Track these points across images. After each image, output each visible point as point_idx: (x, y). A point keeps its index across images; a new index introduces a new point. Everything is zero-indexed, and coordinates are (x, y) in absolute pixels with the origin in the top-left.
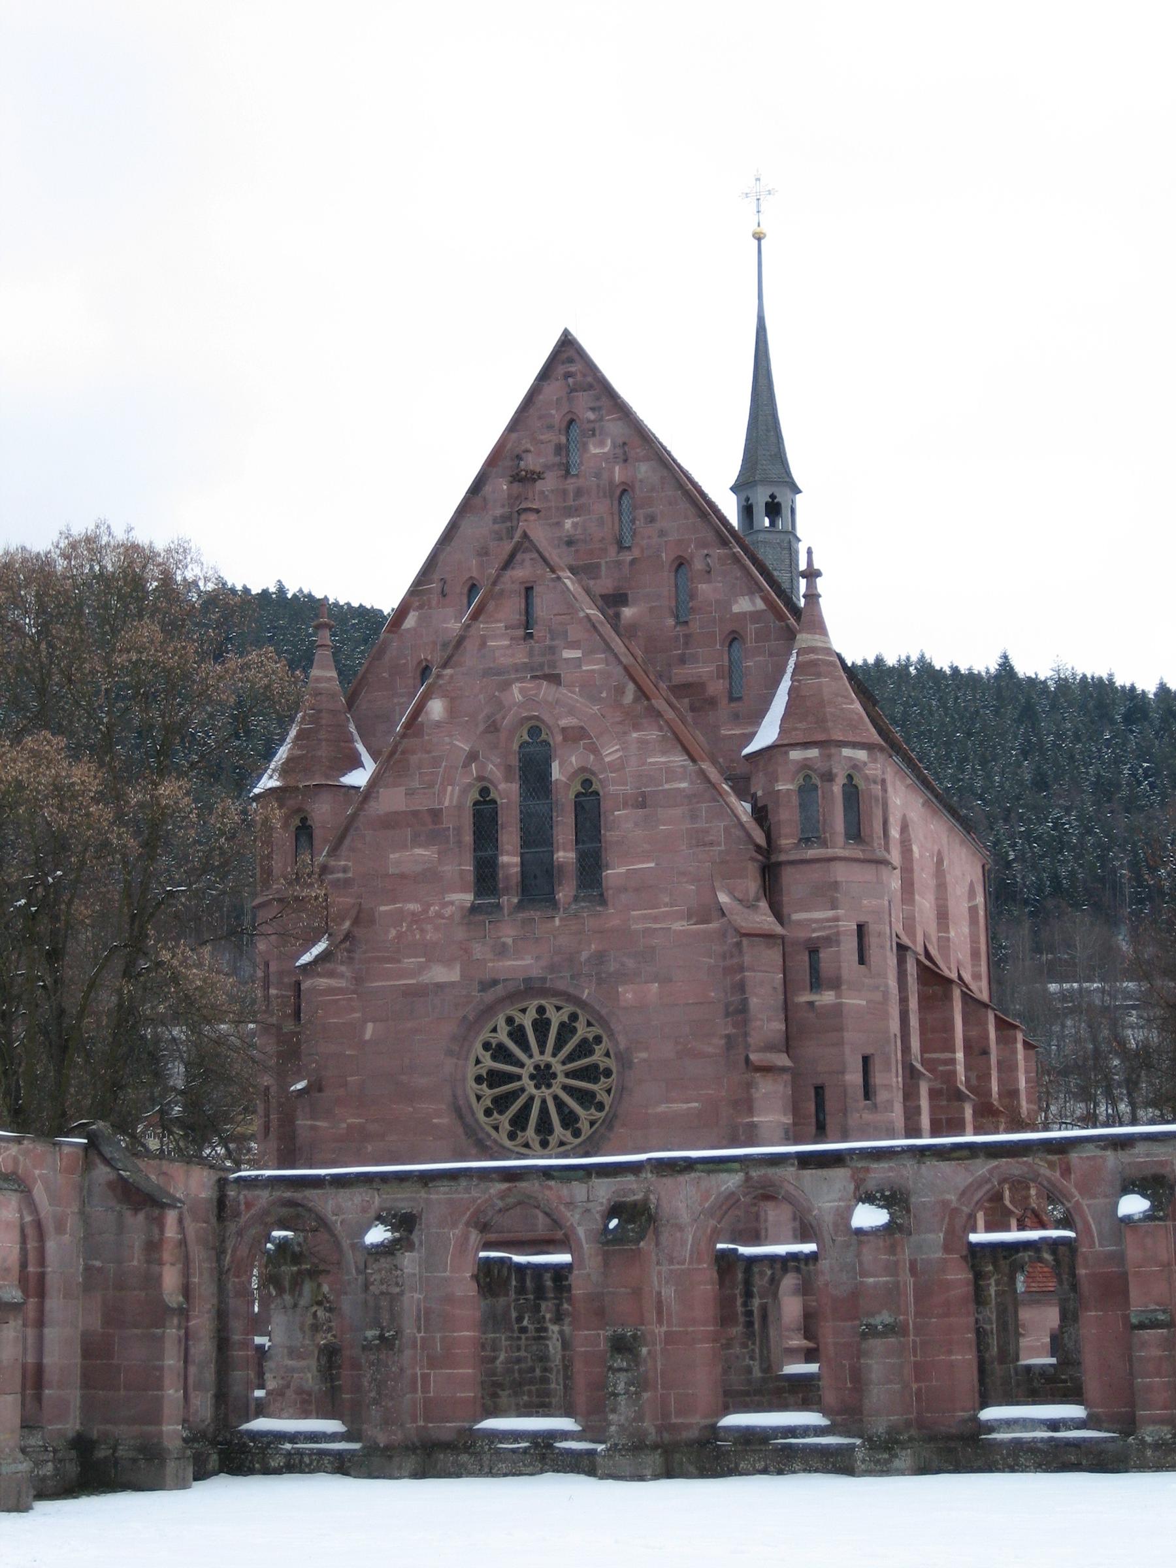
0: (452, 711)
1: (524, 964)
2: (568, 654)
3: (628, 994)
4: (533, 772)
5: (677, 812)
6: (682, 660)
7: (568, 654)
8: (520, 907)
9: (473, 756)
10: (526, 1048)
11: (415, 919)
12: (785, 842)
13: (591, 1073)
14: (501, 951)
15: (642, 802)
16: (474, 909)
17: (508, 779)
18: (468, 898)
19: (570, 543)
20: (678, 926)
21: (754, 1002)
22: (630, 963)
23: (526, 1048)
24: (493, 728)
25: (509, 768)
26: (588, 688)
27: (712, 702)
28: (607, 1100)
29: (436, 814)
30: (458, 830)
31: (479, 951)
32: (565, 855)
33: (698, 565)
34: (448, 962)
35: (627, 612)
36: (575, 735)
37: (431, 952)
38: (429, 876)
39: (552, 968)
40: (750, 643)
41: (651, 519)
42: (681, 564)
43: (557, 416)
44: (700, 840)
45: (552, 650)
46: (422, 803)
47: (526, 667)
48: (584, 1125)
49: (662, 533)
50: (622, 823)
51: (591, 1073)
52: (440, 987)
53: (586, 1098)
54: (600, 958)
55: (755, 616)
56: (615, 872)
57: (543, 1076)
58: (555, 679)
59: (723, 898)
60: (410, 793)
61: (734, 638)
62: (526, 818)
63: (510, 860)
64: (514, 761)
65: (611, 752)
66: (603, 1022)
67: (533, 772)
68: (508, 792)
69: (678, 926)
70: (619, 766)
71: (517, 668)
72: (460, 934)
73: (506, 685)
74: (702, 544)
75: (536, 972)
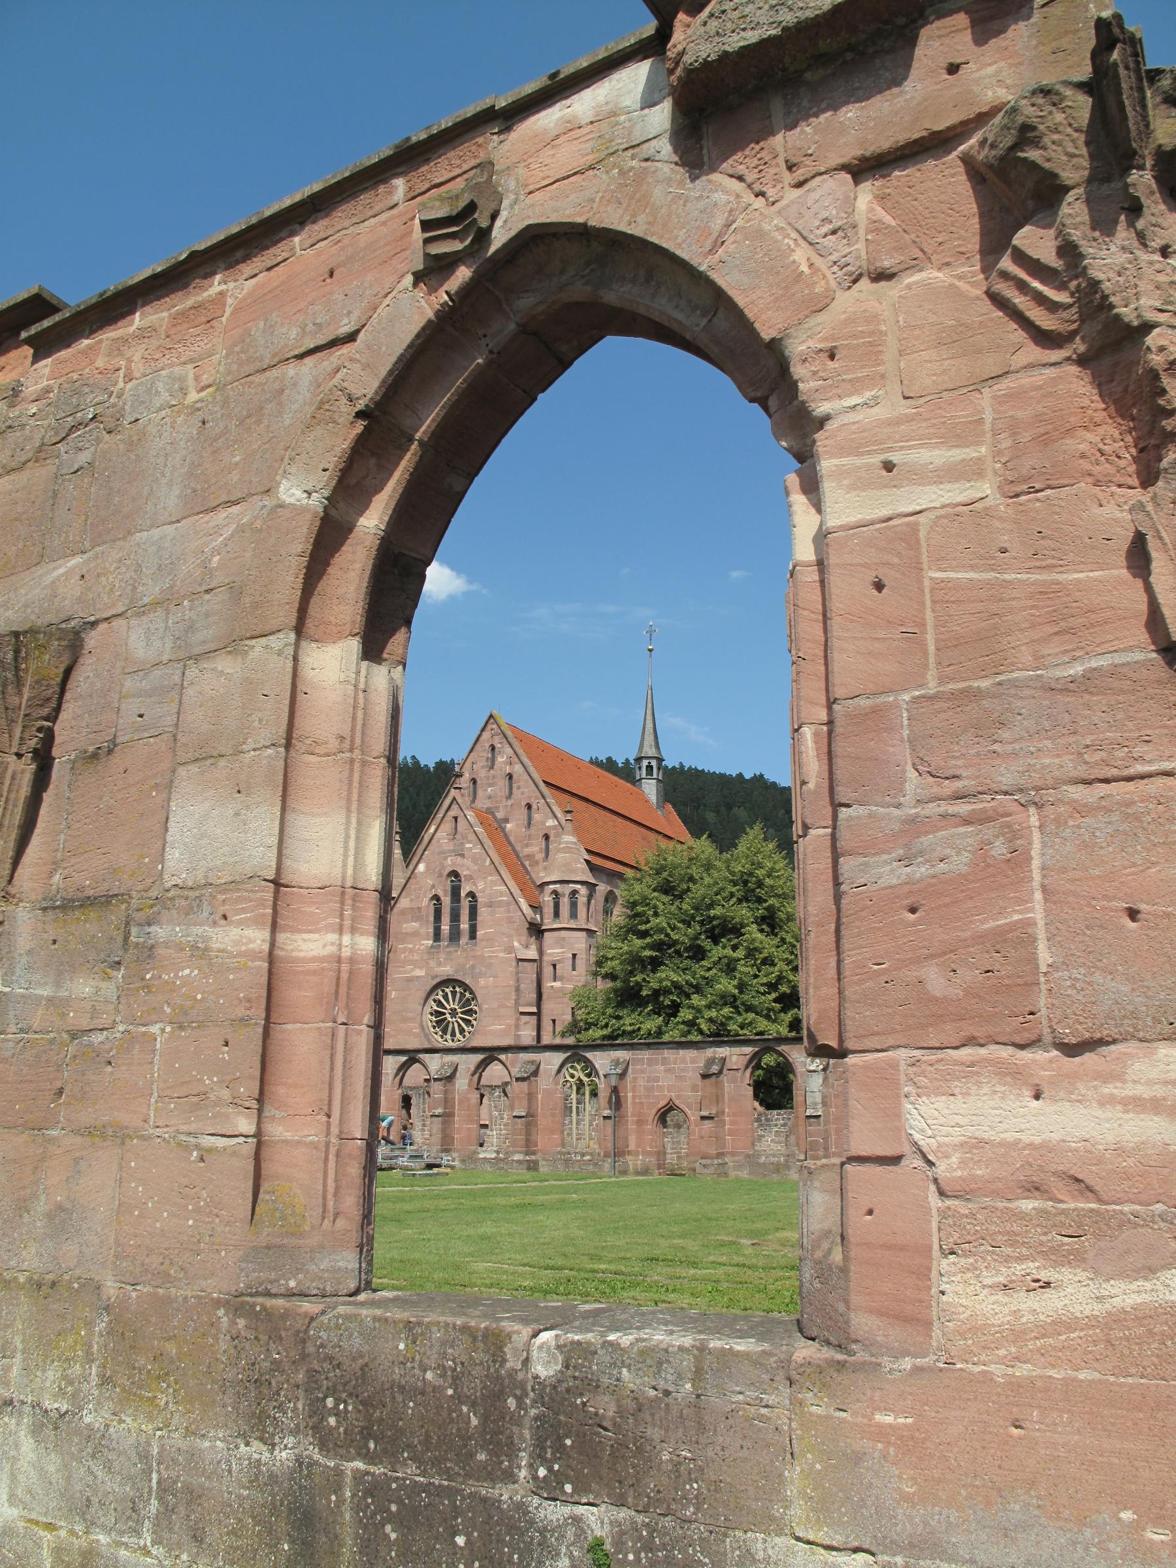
0: (427, 868)
1: (446, 970)
2: (468, 846)
3: (482, 982)
4: (455, 892)
5: (502, 909)
6: (527, 845)
7: (468, 846)
8: (447, 946)
9: (433, 886)
10: (448, 1002)
11: (411, 951)
12: (546, 921)
13: (470, 1012)
14: (439, 964)
15: (490, 905)
16: (432, 947)
17: (445, 895)
18: (431, 942)
19: (490, 798)
20: (501, 955)
21: (522, 986)
22: (483, 969)
23: (448, 1002)
24: (440, 875)
25: (445, 891)
26: (475, 859)
27: (537, 863)
28: (474, 1023)
29: (419, 909)
30: (427, 916)
31: (432, 963)
32: (465, 926)
33: (534, 807)
34: (421, 968)
35: (509, 826)
36: (469, 878)
37: (415, 964)
38: (416, 934)
39: (456, 971)
40: (551, 839)
41: (519, 788)
42: (529, 806)
43: (487, 745)
44: (510, 921)
45: (462, 844)
46: (415, 905)
47: (454, 851)
48: (467, 1034)
49: (522, 793)
50: (483, 912)
51: (470, 1012)
52: (418, 977)
53: (468, 1022)
54: (473, 967)
55: (554, 827)
56: (480, 933)
57: (453, 1013)
58: (463, 856)
59: (516, 944)
60: (411, 900)
61: (547, 837)
62: (452, 909)
63: (445, 928)
64: (449, 888)
65: (481, 885)
66: (472, 992)
67: (455, 892)
68: (446, 901)
69: (501, 955)
70: (483, 891)
71: (450, 851)
72: (426, 957)
73: (446, 858)
74: (536, 798)
75: (451, 973)
